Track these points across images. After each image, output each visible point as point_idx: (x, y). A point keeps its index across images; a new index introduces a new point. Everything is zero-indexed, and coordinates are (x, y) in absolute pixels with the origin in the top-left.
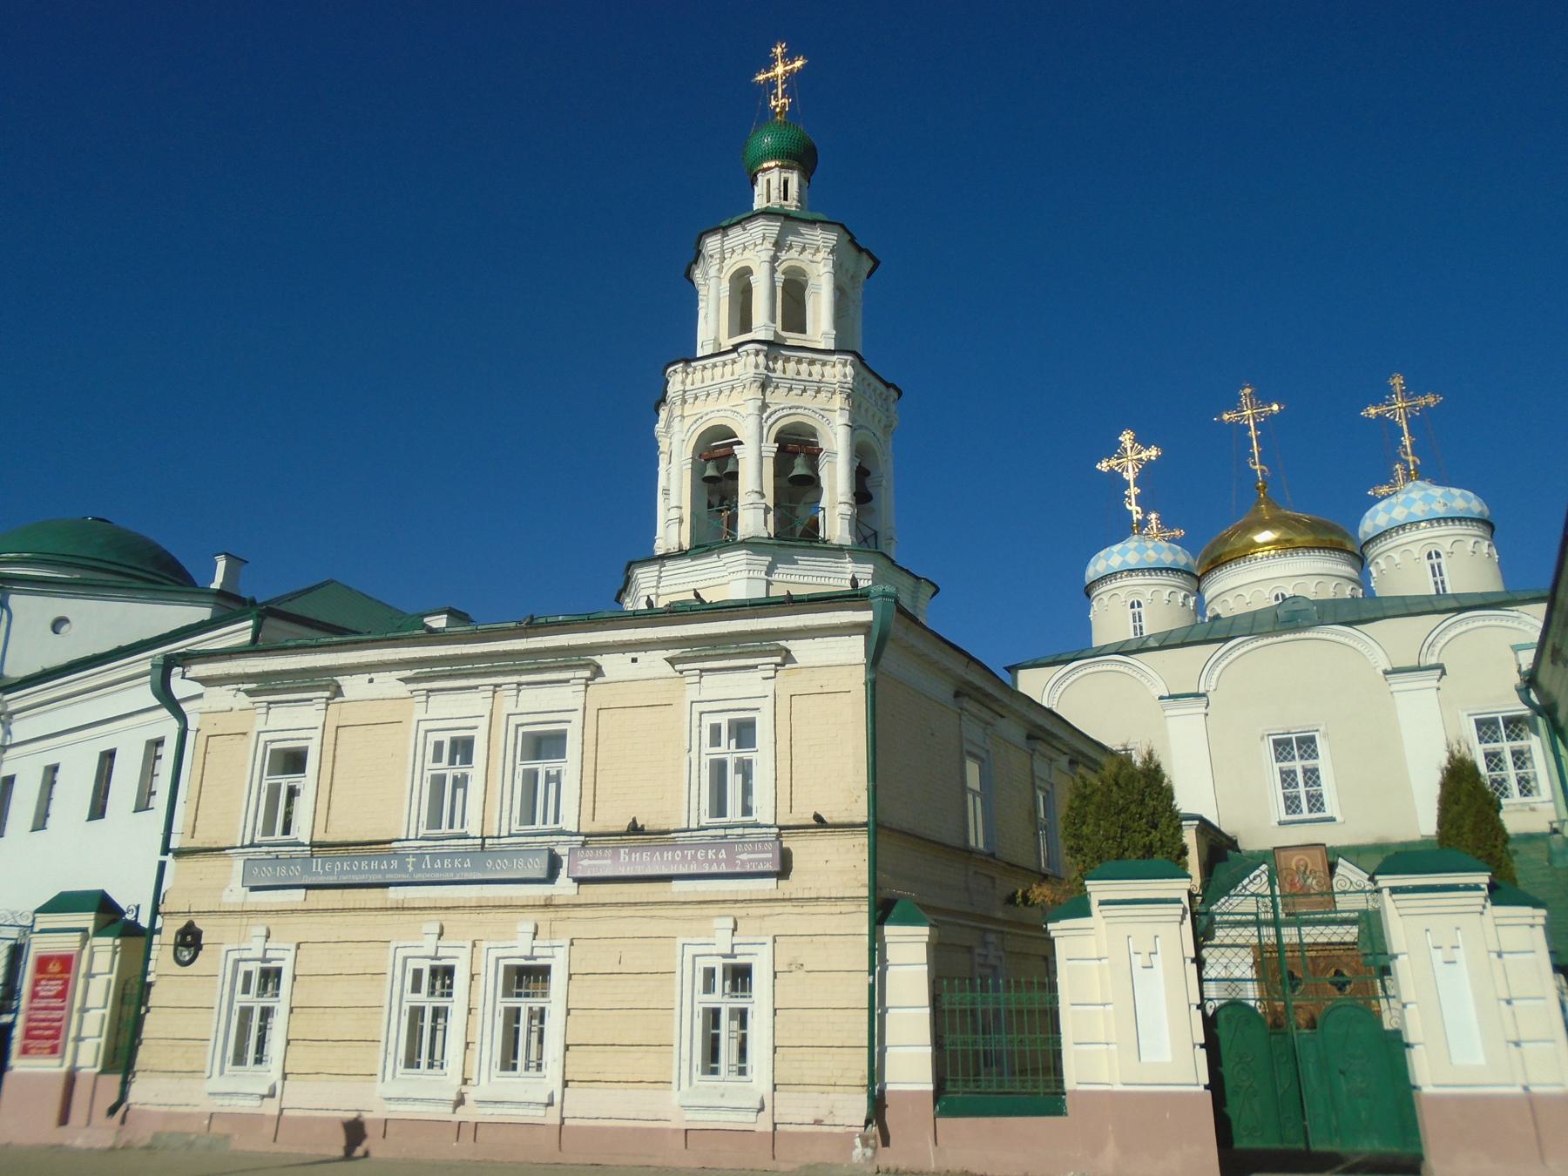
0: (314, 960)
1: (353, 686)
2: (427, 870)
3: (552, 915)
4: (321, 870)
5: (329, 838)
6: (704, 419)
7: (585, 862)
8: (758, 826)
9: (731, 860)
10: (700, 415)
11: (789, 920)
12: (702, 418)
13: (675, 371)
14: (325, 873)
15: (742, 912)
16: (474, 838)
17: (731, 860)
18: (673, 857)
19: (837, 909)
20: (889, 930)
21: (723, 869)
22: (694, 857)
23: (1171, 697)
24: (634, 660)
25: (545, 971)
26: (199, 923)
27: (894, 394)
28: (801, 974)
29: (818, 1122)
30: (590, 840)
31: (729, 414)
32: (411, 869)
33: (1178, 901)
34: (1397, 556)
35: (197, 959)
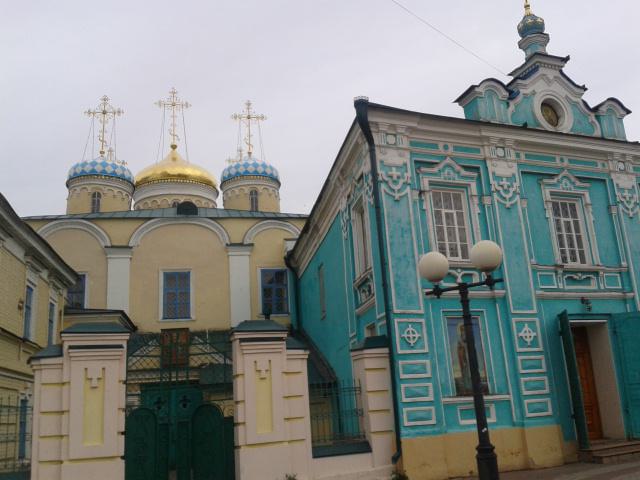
23: (112, 247)
34: (237, 190)
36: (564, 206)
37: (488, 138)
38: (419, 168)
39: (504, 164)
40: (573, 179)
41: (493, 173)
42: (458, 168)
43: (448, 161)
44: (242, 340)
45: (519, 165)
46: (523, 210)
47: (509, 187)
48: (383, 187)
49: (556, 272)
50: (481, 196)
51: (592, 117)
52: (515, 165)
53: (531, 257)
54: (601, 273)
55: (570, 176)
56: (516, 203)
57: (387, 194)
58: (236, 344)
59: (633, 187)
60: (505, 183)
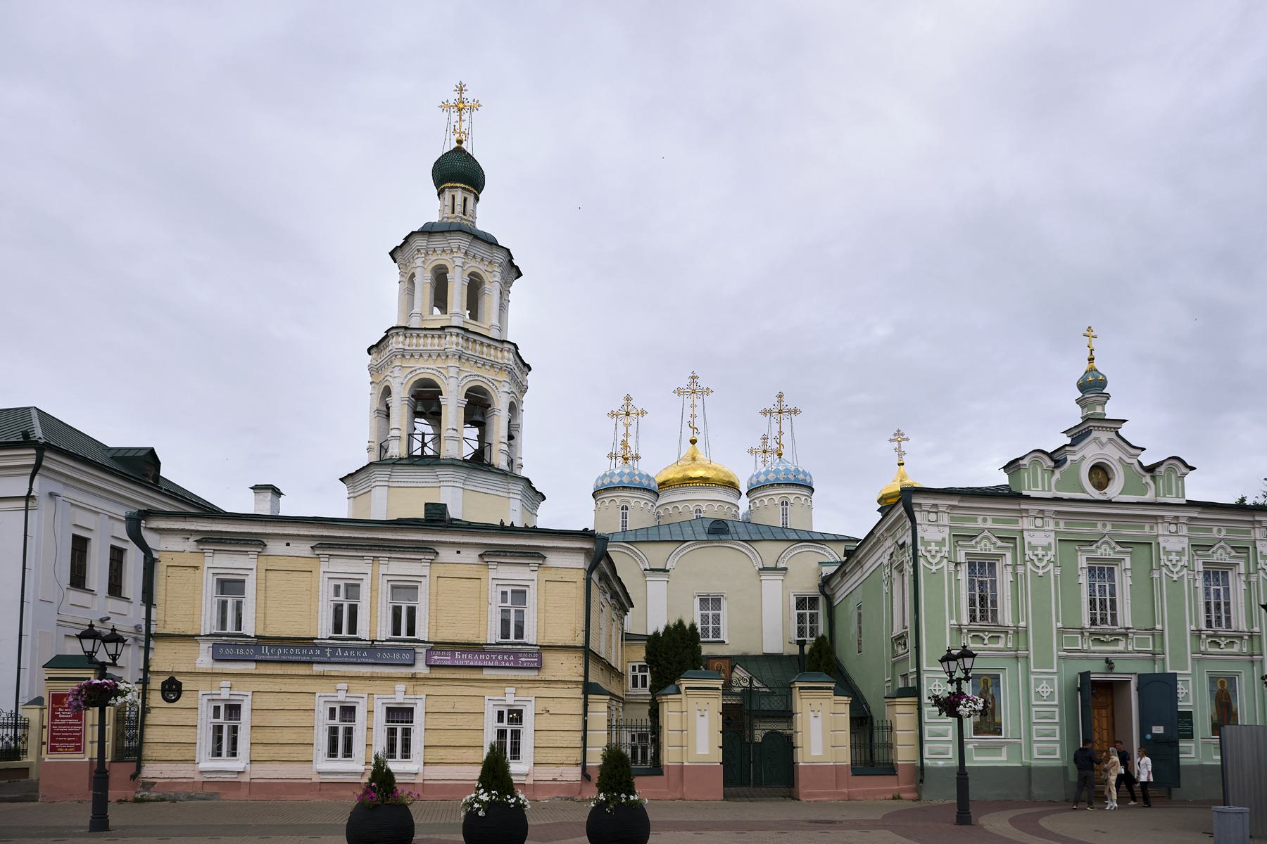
2: (339, 656)
3: (415, 683)
6: (418, 371)
7: (436, 657)
8: (527, 644)
9: (517, 659)
10: (413, 369)
11: (544, 691)
12: (415, 370)
13: (397, 333)
14: (271, 654)
15: (520, 686)
16: (365, 640)
17: (516, 661)
18: (485, 657)
20: (590, 696)
21: (512, 664)
22: (497, 658)
24: (458, 552)
25: (410, 711)
28: (547, 715)
29: (554, 780)
30: (438, 646)
31: (433, 372)
32: (329, 655)
36: (1102, 571)
37: (1027, 510)
38: (957, 542)
39: (1042, 534)
40: (1114, 544)
41: (1029, 543)
42: (994, 539)
43: (986, 533)
44: (801, 688)
45: (1056, 533)
46: (1056, 577)
47: (1043, 556)
48: (922, 562)
49: (1082, 633)
50: (1015, 566)
51: (1147, 478)
52: (1053, 534)
53: (1057, 621)
54: (1131, 635)
55: (1110, 540)
56: (1050, 570)
57: (924, 565)
58: (796, 692)
59: (1183, 549)
60: (1040, 552)
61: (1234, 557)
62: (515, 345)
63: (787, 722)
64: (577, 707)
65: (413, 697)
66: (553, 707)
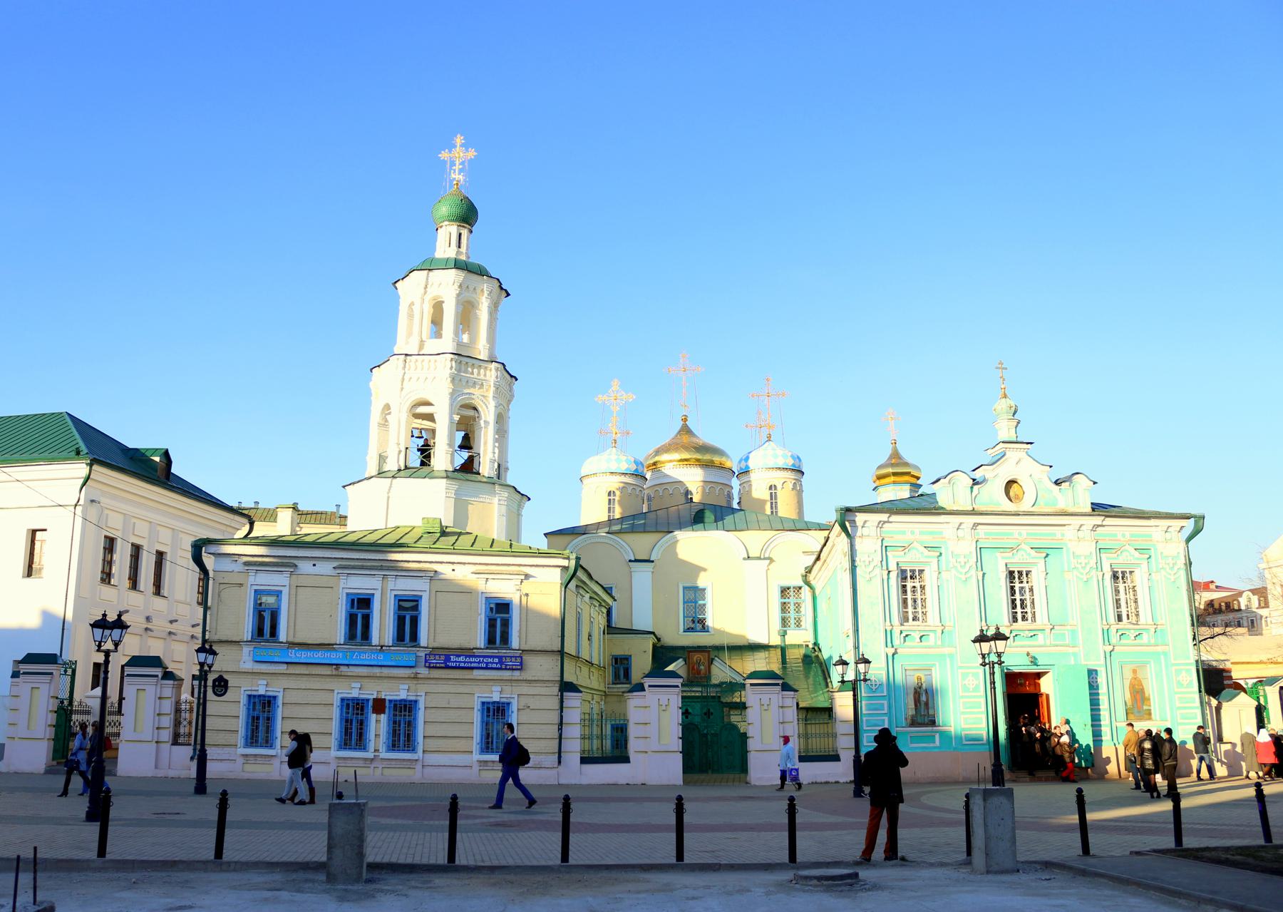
0: (293, 697)
1: (305, 567)
4: (295, 655)
5: (297, 640)
11: (525, 689)
17: (501, 662)
19: (545, 685)
20: (565, 694)
26: (226, 677)
27: (514, 379)
28: (528, 710)
33: (677, 686)
35: (227, 693)
44: (752, 685)
61: (1138, 559)
62: (503, 364)
63: (741, 714)
64: (555, 703)
65: (414, 694)
66: (533, 703)
